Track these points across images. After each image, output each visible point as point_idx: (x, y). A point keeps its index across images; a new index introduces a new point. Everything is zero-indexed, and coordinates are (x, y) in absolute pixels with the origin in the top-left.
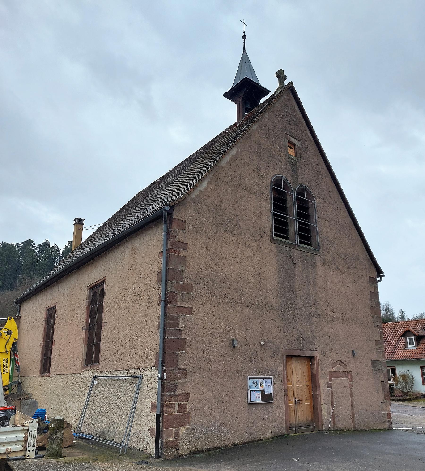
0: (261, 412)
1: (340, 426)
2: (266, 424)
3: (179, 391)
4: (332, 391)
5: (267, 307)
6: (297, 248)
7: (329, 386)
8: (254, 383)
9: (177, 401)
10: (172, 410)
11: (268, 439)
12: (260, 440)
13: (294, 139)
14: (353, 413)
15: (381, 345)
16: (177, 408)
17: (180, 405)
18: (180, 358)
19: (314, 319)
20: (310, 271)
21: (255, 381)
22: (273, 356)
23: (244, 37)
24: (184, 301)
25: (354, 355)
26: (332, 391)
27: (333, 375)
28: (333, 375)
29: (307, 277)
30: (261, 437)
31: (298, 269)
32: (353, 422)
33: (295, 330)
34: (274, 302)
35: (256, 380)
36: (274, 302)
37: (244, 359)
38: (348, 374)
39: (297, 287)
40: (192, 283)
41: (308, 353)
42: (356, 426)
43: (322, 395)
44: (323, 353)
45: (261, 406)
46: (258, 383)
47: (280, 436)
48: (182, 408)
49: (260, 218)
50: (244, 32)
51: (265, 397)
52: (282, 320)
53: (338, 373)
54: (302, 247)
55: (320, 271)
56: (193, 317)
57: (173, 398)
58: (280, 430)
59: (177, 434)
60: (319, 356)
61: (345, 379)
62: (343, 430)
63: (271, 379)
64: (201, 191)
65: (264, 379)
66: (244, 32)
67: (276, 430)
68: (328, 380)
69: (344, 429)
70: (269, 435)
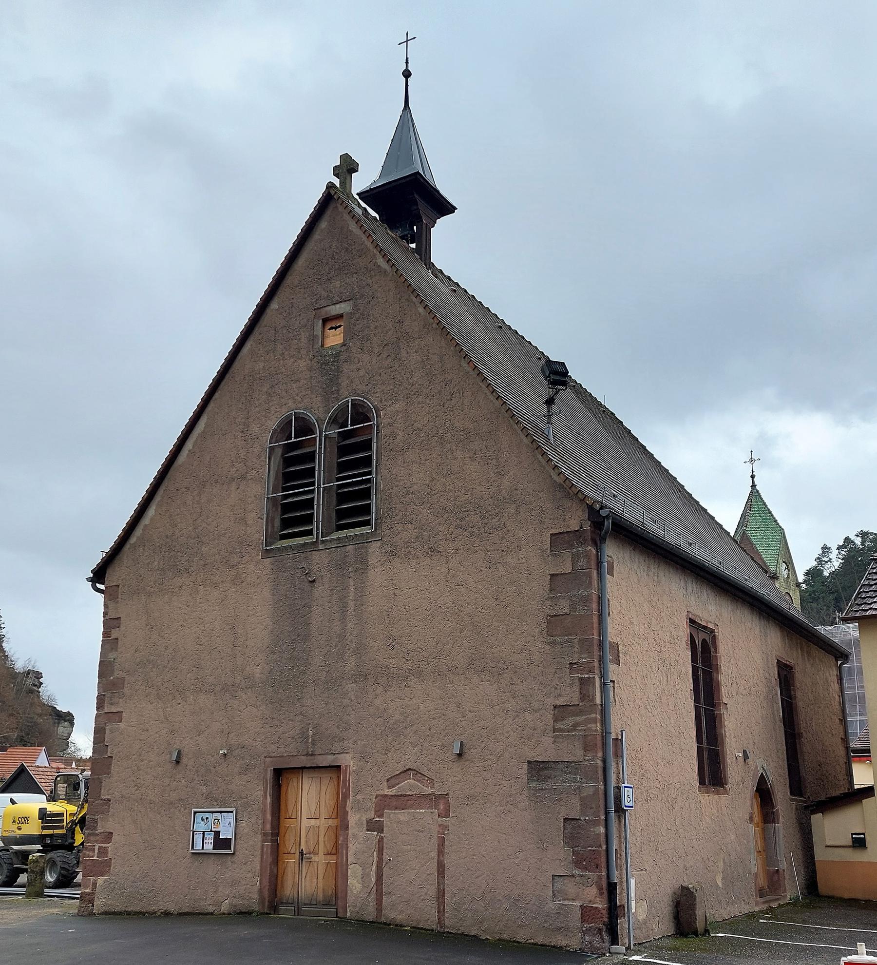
0: (211, 868)
1: (392, 914)
2: (220, 889)
3: (100, 830)
4: (381, 840)
5: (243, 685)
6: (321, 547)
7: (374, 826)
8: (203, 820)
9: (97, 841)
10: (91, 854)
11: (224, 914)
12: (208, 914)
13: (338, 306)
14: (441, 895)
15: (579, 719)
16: (96, 851)
17: (100, 848)
18: (103, 784)
19: (350, 686)
20: (351, 582)
21: (205, 816)
22: (245, 770)
23: (407, 74)
24: (112, 704)
25: (177, 762)
26: (381, 840)
27: (384, 803)
28: (384, 803)
29: (343, 600)
30: (211, 909)
31: (320, 590)
32: (441, 911)
33: (299, 718)
34: (257, 673)
35: (207, 815)
36: (257, 673)
37: (192, 780)
38: (435, 799)
39: (313, 628)
40: (124, 675)
41: (327, 761)
42: (447, 922)
43: (350, 845)
44: (364, 757)
45: (213, 857)
46: (210, 819)
47: (245, 913)
48: (103, 852)
49: (244, 520)
50: (407, 63)
51: (221, 843)
52: (271, 702)
53: (406, 798)
54: (331, 541)
55: (378, 576)
56: (122, 725)
57: (92, 838)
58: (246, 902)
59: (95, 884)
60: (352, 764)
61: (427, 816)
62: (401, 926)
63: (195, 813)
64: (146, 525)
65: (221, 812)
66: (407, 63)
67: (238, 902)
68: (371, 814)
69: (404, 923)
70: (225, 908)
